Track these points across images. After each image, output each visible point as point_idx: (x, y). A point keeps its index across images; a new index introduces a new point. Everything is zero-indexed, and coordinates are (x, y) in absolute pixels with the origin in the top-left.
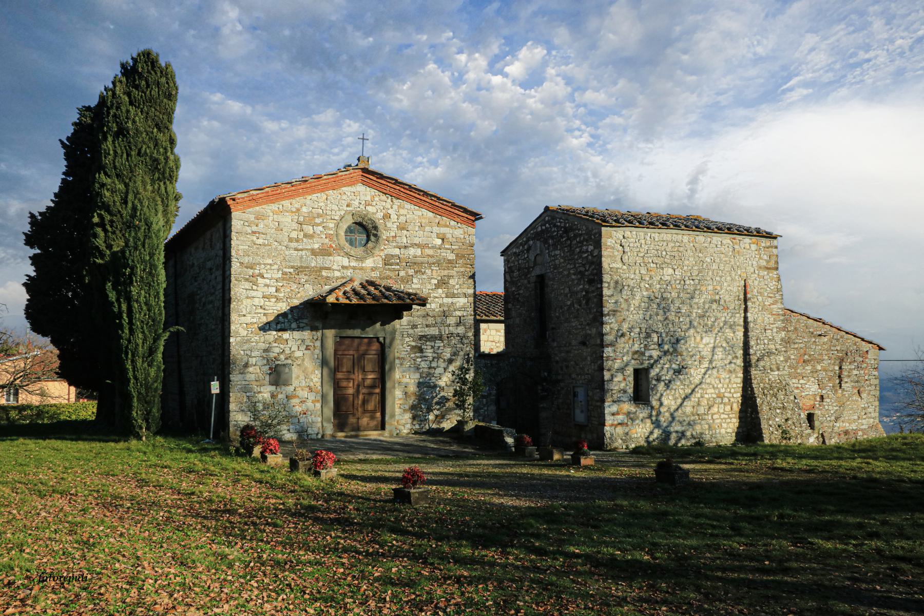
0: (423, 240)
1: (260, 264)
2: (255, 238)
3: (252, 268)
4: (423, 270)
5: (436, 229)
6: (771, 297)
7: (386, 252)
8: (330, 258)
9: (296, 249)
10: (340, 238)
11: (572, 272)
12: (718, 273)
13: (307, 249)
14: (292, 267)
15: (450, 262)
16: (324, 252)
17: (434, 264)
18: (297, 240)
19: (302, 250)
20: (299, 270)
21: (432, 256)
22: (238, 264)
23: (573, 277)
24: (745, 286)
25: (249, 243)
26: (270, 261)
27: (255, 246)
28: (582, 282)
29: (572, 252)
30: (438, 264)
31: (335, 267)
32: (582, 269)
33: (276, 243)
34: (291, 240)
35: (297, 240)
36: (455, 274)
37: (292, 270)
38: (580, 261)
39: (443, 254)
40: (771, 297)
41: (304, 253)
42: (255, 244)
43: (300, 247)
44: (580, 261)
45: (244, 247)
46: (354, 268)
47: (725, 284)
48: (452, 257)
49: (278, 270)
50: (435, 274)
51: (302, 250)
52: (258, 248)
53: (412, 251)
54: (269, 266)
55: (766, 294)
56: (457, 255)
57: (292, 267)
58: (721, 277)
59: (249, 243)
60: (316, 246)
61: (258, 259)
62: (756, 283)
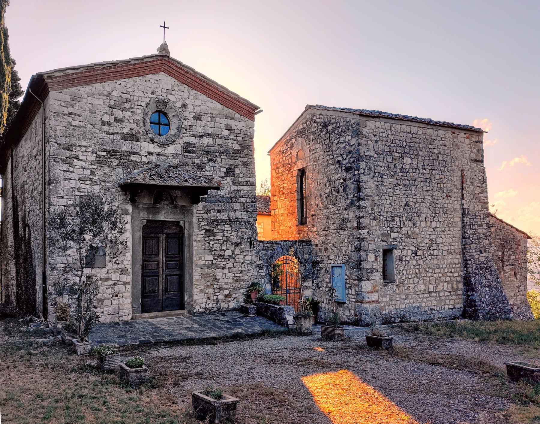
0: (214, 131)
1: (76, 146)
2: (71, 119)
3: (68, 150)
4: (215, 159)
5: (225, 121)
6: (479, 187)
7: (185, 140)
8: (138, 143)
9: (108, 133)
10: (146, 124)
11: (330, 162)
12: (442, 164)
13: (118, 133)
14: (105, 151)
15: (236, 152)
16: (132, 137)
17: (223, 153)
18: (109, 124)
19: (113, 134)
20: (112, 153)
21: (221, 146)
22: (56, 145)
23: (332, 167)
24: (462, 176)
25: (66, 124)
26: (84, 143)
27: (71, 128)
28: (340, 170)
29: (331, 144)
30: (226, 152)
31: (141, 153)
32: (340, 159)
33: (90, 126)
34: (103, 123)
35: (109, 124)
36: (240, 163)
37: (105, 153)
38: (338, 152)
39: (230, 145)
40: (479, 187)
41: (115, 137)
42: (71, 125)
43: (111, 131)
44: (338, 152)
45: (61, 128)
46: (158, 154)
47: (448, 174)
48: (237, 147)
49: (92, 153)
50: (223, 162)
51: (113, 134)
52: (74, 130)
53: (206, 141)
54: (84, 149)
55: (475, 184)
56: (241, 146)
57: (105, 151)
58: (445, 167)
59: (66, 124)
60: (126, 131)
61: (74, 141)
62: (469, 173)
